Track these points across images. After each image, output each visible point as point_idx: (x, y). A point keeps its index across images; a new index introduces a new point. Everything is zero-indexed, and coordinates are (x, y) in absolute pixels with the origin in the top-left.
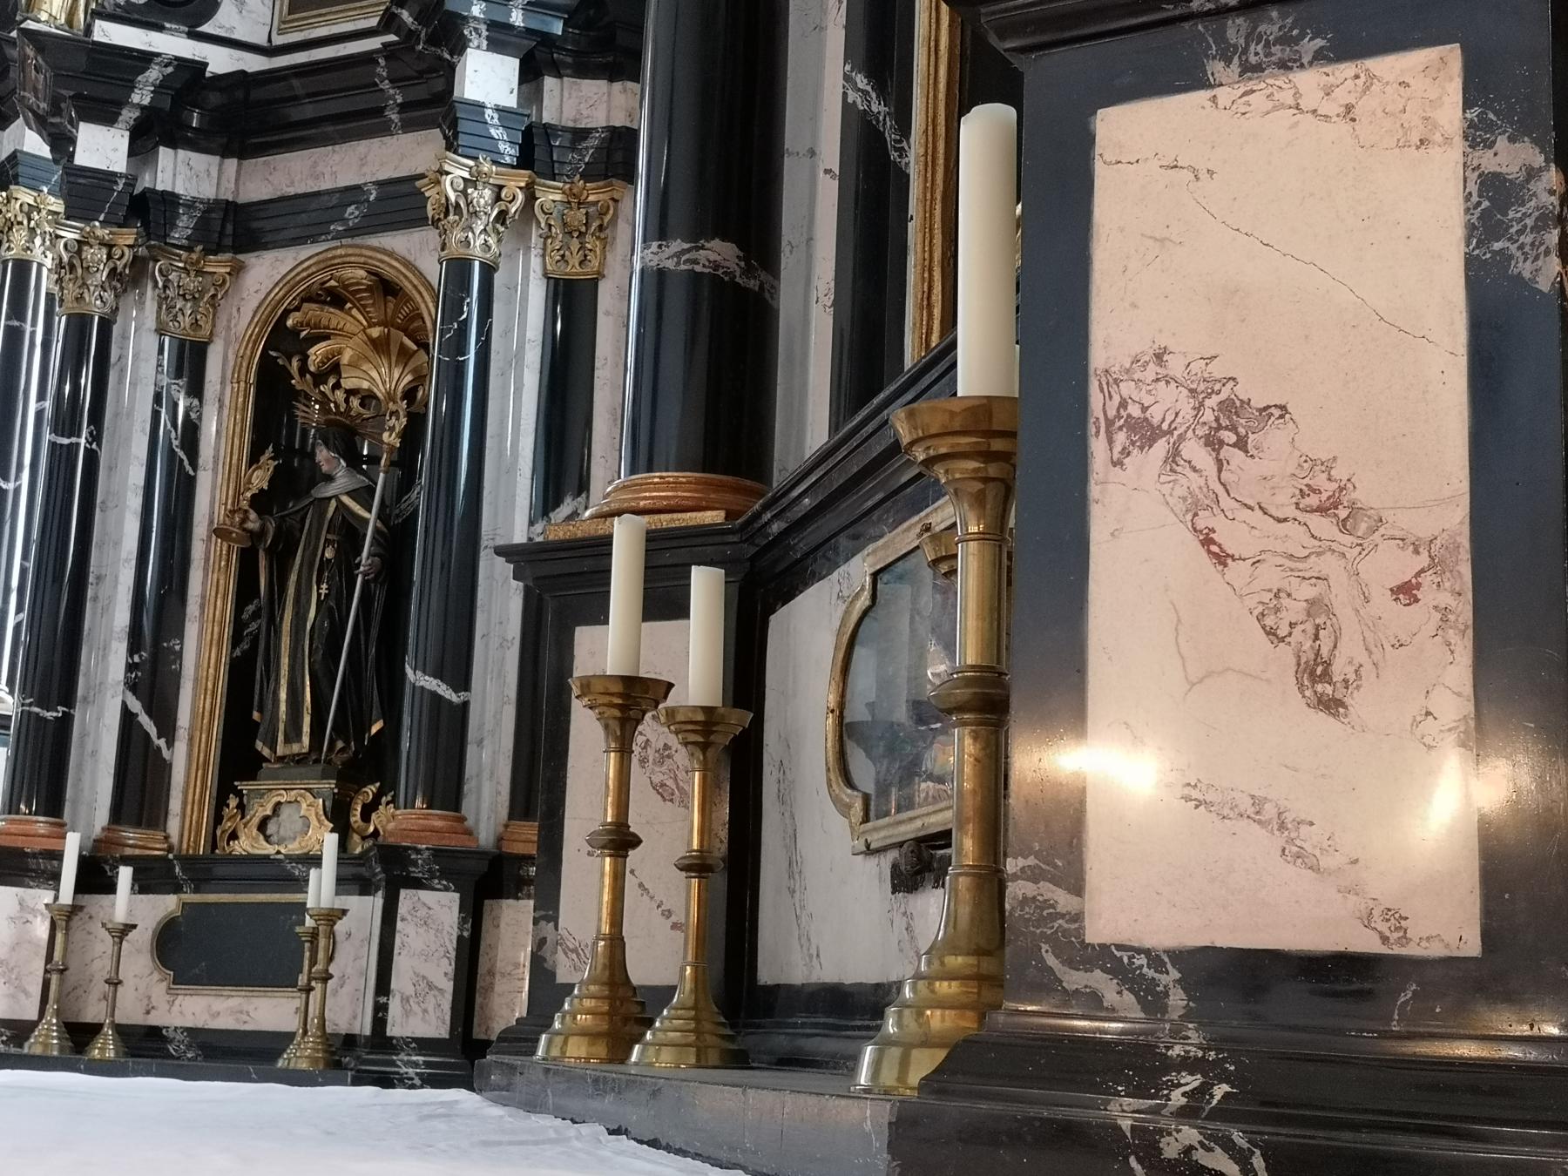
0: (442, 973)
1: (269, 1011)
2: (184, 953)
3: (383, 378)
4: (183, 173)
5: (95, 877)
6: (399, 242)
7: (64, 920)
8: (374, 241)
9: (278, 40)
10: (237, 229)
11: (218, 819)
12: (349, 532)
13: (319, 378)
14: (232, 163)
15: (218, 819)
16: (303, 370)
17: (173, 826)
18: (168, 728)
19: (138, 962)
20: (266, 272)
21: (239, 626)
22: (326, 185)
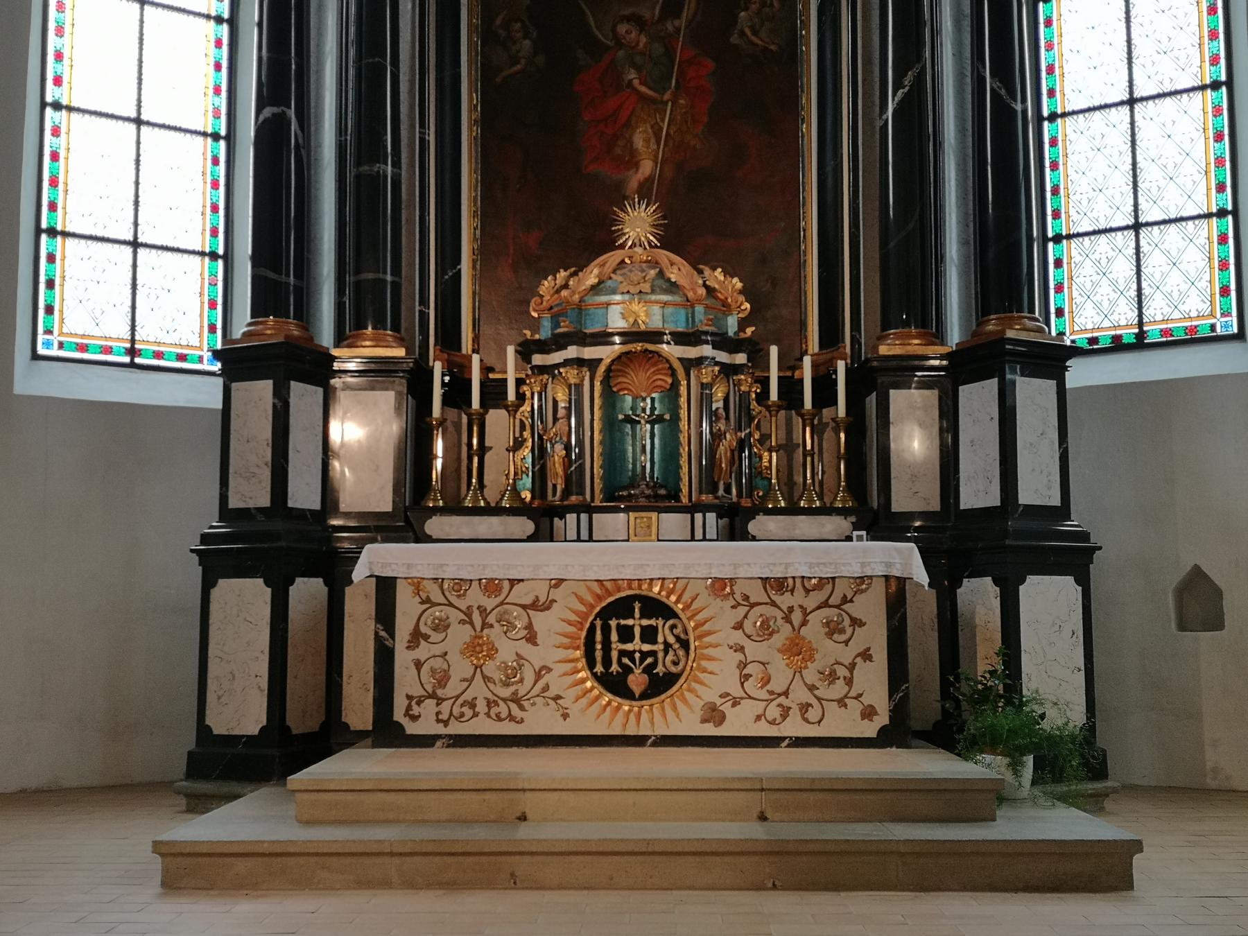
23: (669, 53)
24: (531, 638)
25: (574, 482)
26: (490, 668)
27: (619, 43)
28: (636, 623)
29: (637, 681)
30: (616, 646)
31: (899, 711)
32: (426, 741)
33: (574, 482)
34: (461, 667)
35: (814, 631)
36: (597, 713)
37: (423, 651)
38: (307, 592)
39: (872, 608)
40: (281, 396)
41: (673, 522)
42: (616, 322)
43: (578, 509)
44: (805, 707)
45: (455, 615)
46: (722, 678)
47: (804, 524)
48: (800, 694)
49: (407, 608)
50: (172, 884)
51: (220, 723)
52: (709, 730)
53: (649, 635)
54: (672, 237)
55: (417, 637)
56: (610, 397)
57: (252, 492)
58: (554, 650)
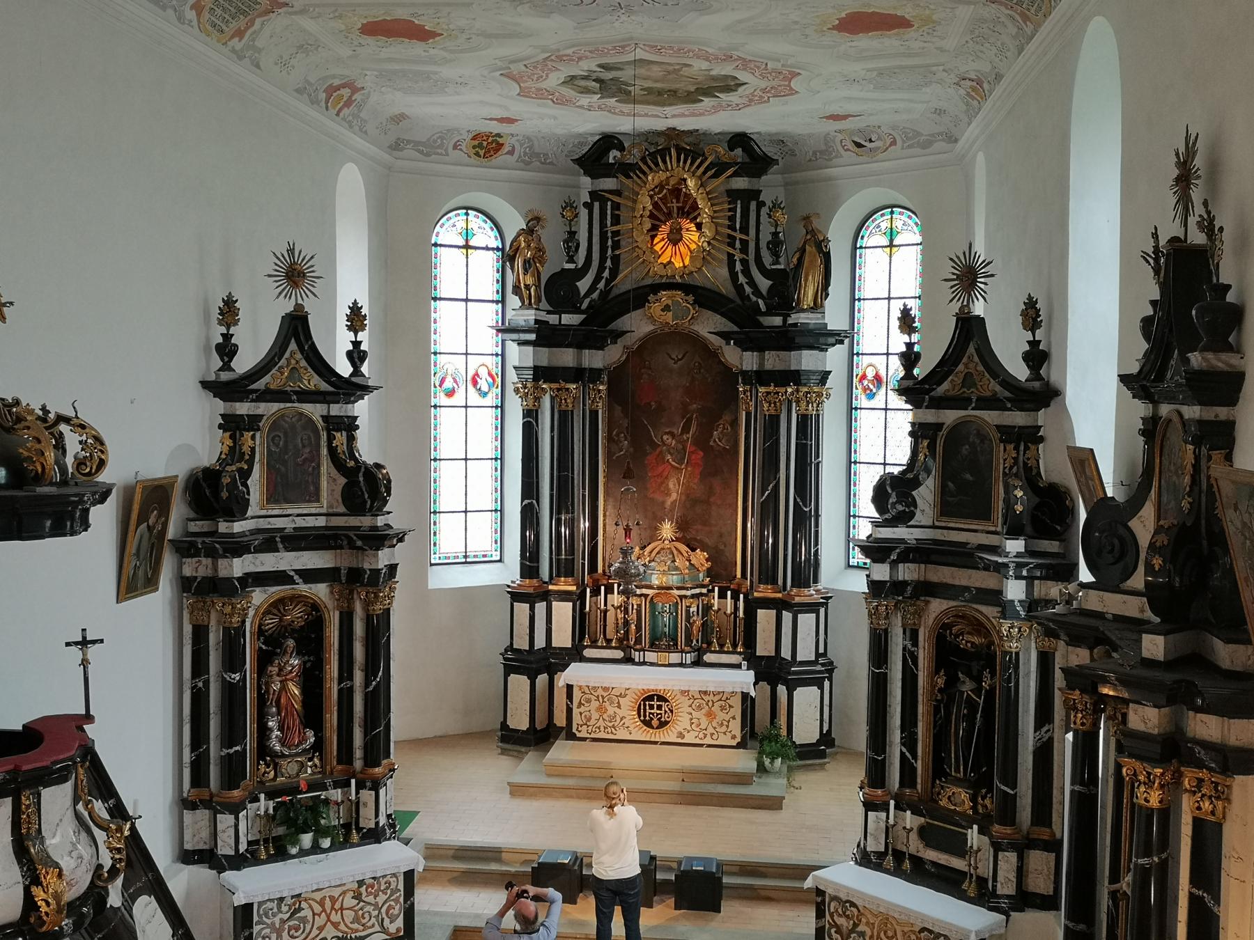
0: (1012, 876)
4: (907, 572)
6: (984, 609)
8: (975, 606)
9: (937, 524)
10: (927, 589)
11: (933, 786)
13: (957, 636)
14: (923, 566)
15: (933, 786)
16: (951, 634)
17: (919, 787)
18: (915, 757)
19: (914, 836)
20: (937, 606)
21: (935, 722)
22: (957, 582)
23: (684, 449)
24: (619, 707)
25: (638, 640)
26: (605, 716)
27: (664, 444)
28: (655, 703)
29: (655, 723)
30: (648, 711)
31: (743, 737)
32: (584, 739)
33: (638, 640)
34: (595, 715)
35: (716, 708)
36: (641, 733)
37: (582, 709)
39: (737, 702)
40: (532, 609)
42: (655, 581)
43: (639, 651)
44: (712, 734)
45: (593, 698)
46: (683, 723)
47: (725, 658)
48: (710, 730)
49: (577, 694)
50: (512, 794)
51: (512, 724)
52: (679, 740)
53: (659, 707)
55: (580, 704)
57: (522, 643)
58: (627, 711)
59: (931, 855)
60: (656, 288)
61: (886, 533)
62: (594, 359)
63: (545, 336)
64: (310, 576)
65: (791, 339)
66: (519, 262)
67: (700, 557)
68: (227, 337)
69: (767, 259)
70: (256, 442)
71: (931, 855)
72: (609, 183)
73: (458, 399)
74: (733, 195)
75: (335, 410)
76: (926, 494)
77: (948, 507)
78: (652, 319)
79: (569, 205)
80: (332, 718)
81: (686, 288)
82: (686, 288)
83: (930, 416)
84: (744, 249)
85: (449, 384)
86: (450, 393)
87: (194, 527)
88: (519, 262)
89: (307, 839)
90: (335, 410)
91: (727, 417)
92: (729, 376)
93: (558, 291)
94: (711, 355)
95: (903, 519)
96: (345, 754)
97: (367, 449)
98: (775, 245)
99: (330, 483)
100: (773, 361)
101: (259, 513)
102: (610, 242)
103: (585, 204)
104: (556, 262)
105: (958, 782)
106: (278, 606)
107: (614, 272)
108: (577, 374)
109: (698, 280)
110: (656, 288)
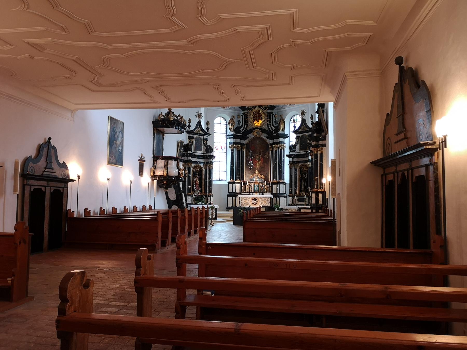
1: (303, 203)
2: (299, 200)
3: (306, 170)
4: (295, 160)
5: (294, 197)
7: (293, 199)
12: (305, 179)
19: (297, 201)
20: (300, 164)
38: (234, 198)
39: (269, 199)
41: (258, 194)
42: (255, 180)
47: (267, 194)
51: (229, 206)
54: (259, 172)
56: (254, 185)
57: (230, 191)
59: (300, 203)
60: (254, 129)
61: (291, 153)
62: (243, 142)
63: (235, 137)
64: (200, 162)
65: (279, 136)
66: (230, 124)
67: (263, 176)
68: (189, 124)
69: (274, 124)
70: (193, 141)
71: (300, 203)
72: (246, 111)
73: (218, 151)
74: (268, 113)
75: (205, 137)
76: (297, 147)
77: (301, 149)
78: (254, 135)
79: (239, 115)
80: (203, 186)
81: (260, 129)
82: (260, 129)
83: (298, 135)
84: (270, 122)
85: (217, 148)
86: (217, 149)
87: (184, 152)
88: (230, 124)
89: (200, 202)
90: (205, 137)
91: (267, 152)
92: (268, 145)
93: (237, 130)
94: (264, 141)
95: (294, 151)
96: (206, 192)
97: (209, 144)
98: (276, 122)
99: (203, 148)
100: (275, 140)
101: (193, 151)
102: (246, 121)
103: (242, 115)
104: (236, 125)
105: (303, 191)
106: (195, 167)
107: (247, 127)
108: (240, 144)
109: (262, 128)
110: (254, 129)
